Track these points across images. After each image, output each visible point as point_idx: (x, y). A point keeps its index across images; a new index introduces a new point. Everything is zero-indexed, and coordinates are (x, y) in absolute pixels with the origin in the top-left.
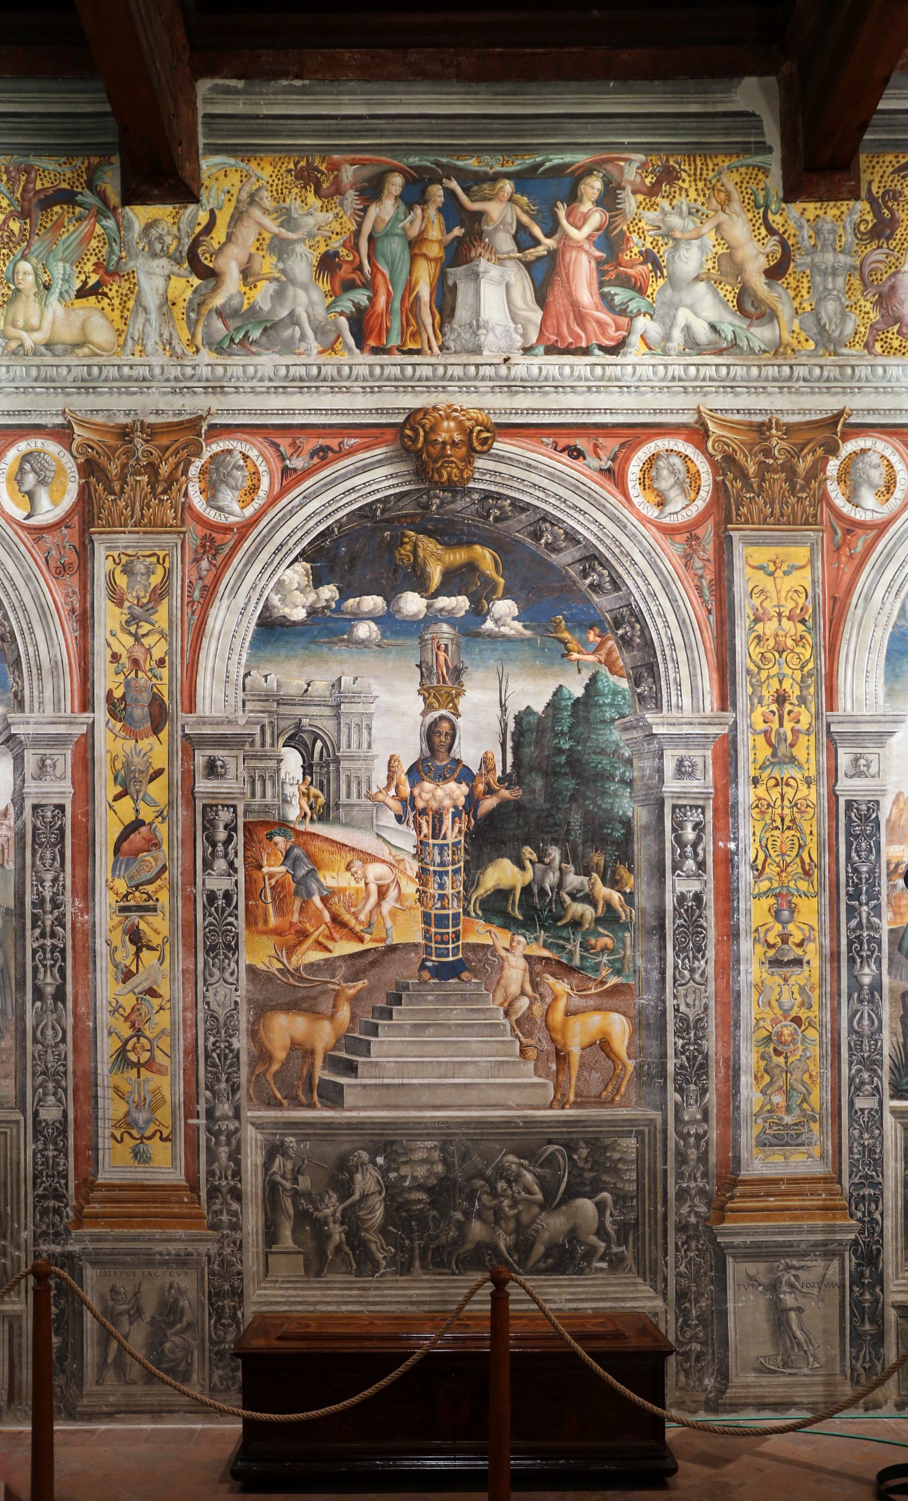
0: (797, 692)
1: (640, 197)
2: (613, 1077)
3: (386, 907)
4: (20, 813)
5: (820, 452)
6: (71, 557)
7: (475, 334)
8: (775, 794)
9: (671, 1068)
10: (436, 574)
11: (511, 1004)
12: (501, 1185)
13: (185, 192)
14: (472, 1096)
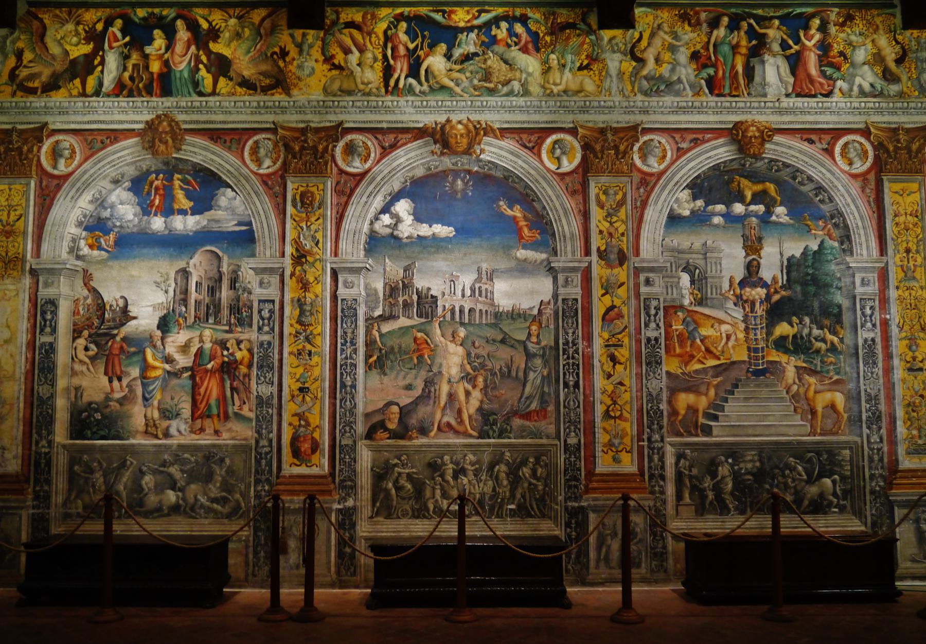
0: (915, 248)
1: (837, 27)
2: (838, 422)
3: (730, 344)
4: (556, 303)
5: (922, 141)
6: (578, 187)
7: (764, 88)
8: (907, 293)
9: (864, 418)
10: (749, 195)
11: (789, 388)
12: (787, 472)
13: (628, 23)
14: (773, 431)
